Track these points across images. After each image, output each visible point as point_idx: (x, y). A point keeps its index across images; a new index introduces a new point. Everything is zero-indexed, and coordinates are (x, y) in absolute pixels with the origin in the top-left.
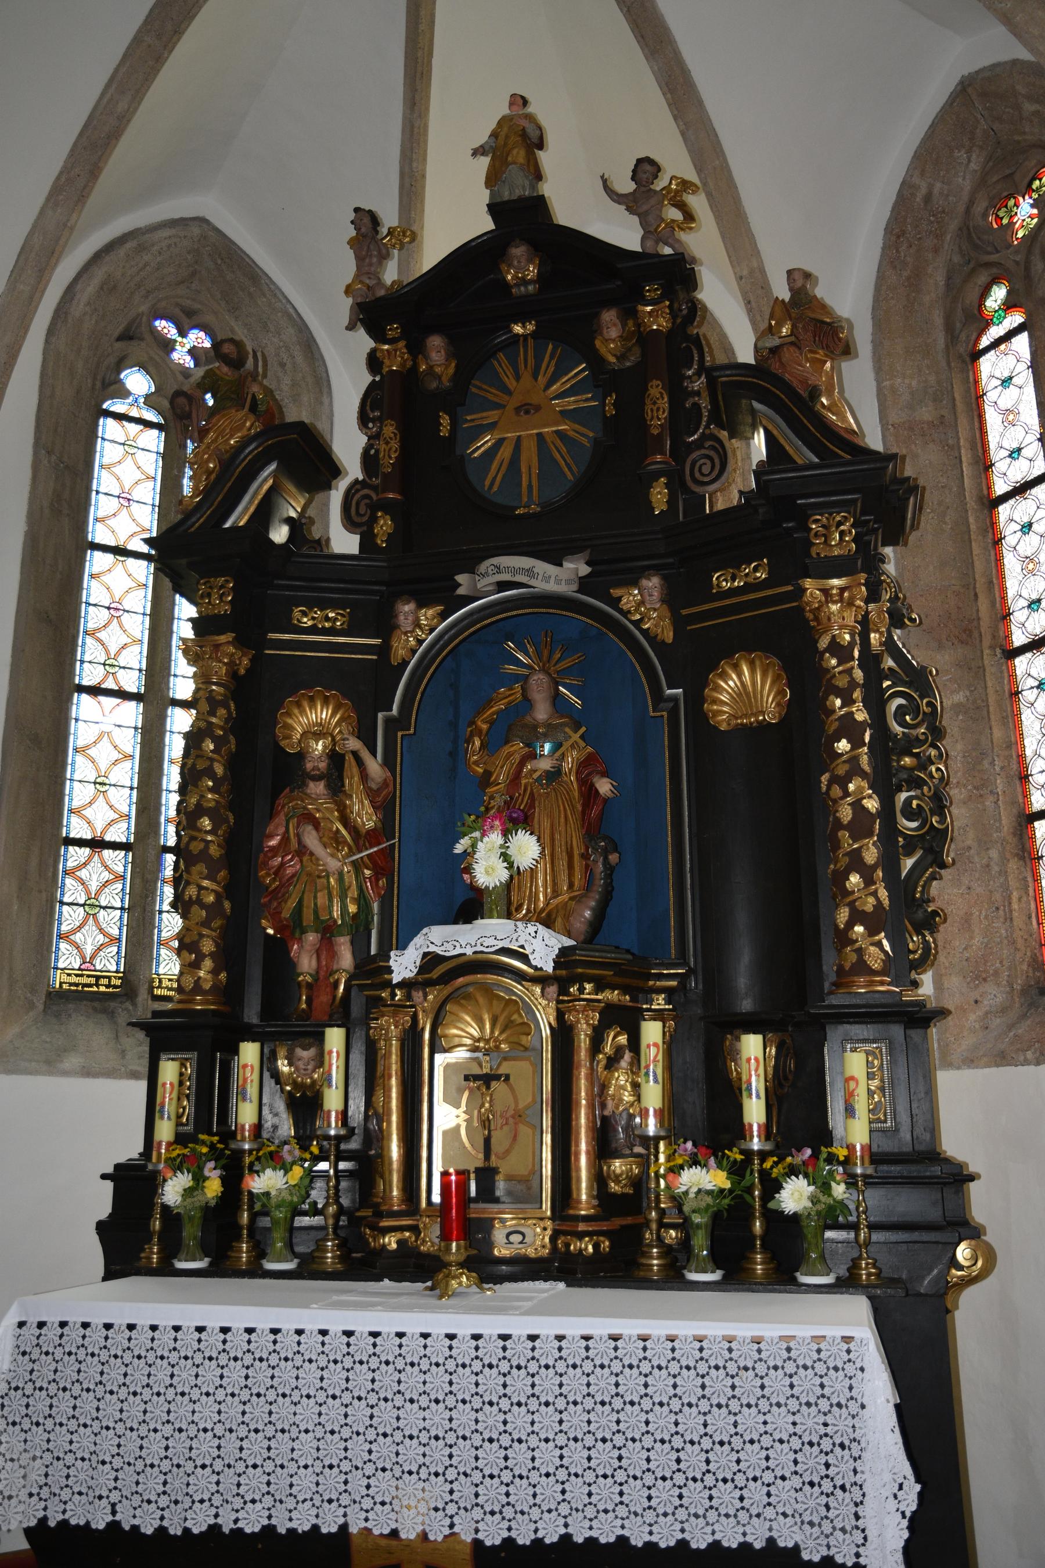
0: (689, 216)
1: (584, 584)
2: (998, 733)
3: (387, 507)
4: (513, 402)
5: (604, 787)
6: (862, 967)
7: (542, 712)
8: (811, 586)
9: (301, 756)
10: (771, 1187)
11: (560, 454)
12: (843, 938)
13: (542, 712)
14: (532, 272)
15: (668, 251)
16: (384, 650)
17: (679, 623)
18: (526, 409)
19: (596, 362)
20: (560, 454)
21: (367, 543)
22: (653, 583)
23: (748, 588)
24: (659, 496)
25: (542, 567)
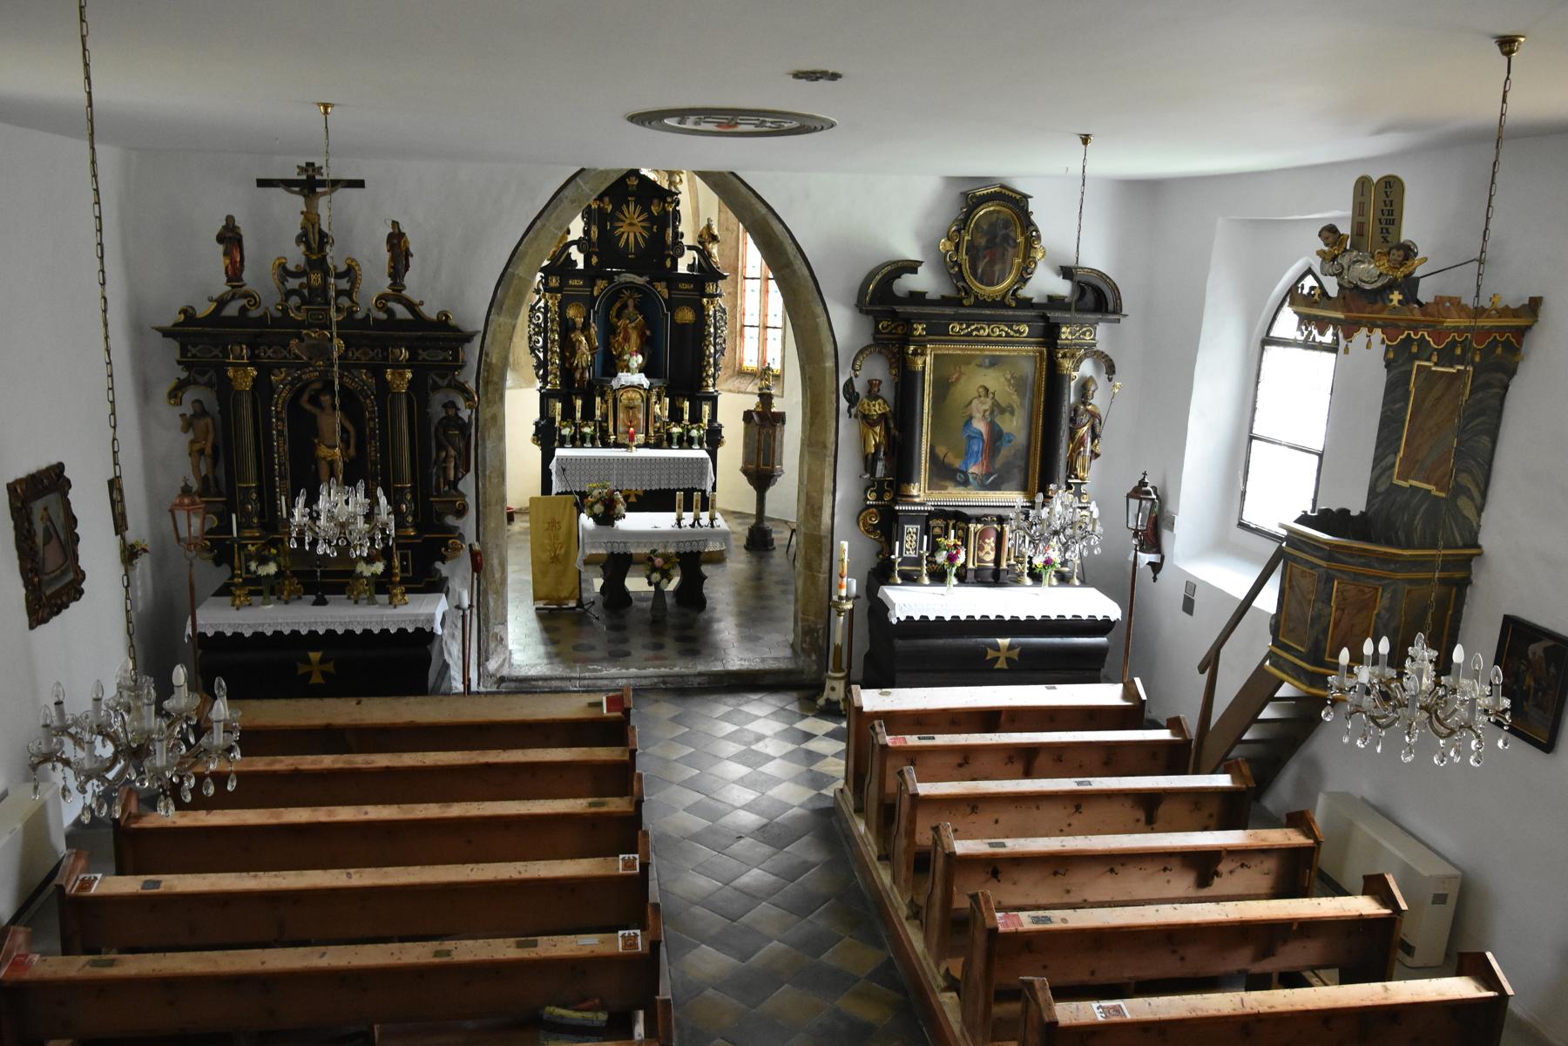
0: (681, 180)
1: (647, 282)
2: (739, 302)
3: (596, 254)
4: (628, 221)
5: (648, 333)
6: (708, 386)
7: (631, 309)
8: (705, 300)
9: (574, 323)
10: (689, 431)
11: (640, 240)
12: (704, 380)
13: (631, 309)
14: (636, 183)
15: (673, 189)
16: (592, 292)
17: (670, 294)
18: (631, 224)
19: (650, 212)
20: (640, 240)
21: (587, 261)
22: (664, 284)
23: (687, 290)
24: (668, 263)
25: (637, 277)
